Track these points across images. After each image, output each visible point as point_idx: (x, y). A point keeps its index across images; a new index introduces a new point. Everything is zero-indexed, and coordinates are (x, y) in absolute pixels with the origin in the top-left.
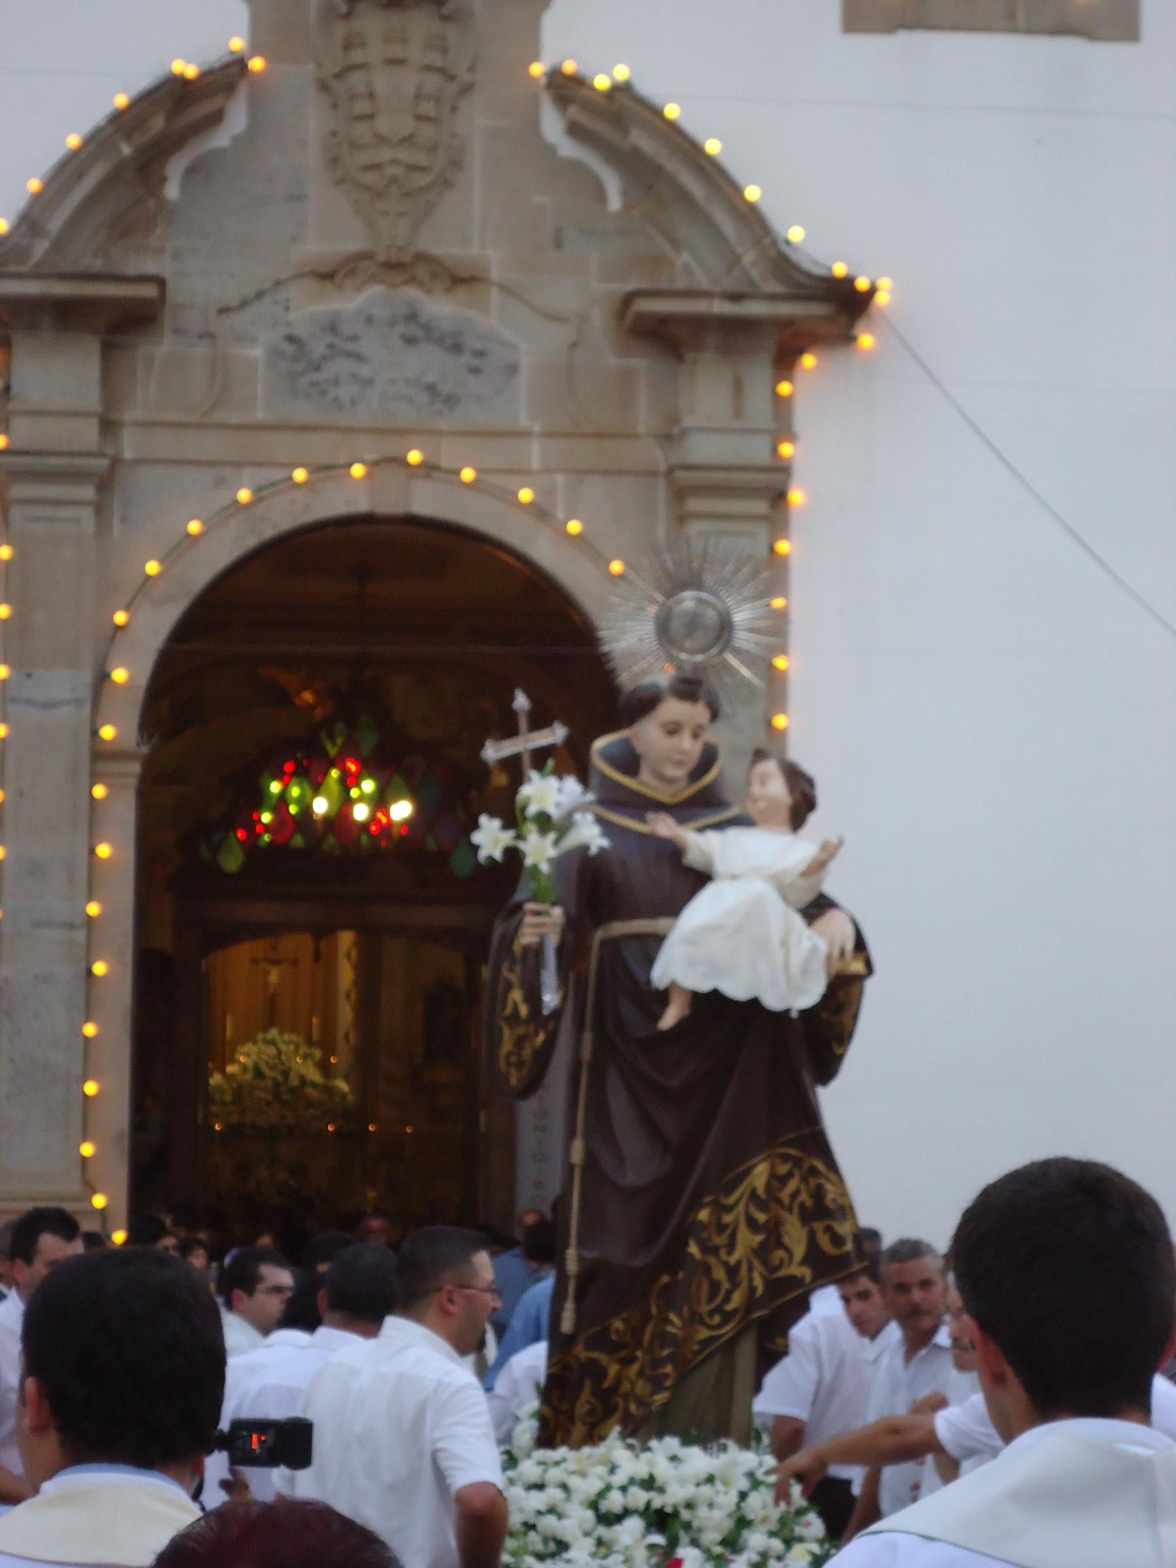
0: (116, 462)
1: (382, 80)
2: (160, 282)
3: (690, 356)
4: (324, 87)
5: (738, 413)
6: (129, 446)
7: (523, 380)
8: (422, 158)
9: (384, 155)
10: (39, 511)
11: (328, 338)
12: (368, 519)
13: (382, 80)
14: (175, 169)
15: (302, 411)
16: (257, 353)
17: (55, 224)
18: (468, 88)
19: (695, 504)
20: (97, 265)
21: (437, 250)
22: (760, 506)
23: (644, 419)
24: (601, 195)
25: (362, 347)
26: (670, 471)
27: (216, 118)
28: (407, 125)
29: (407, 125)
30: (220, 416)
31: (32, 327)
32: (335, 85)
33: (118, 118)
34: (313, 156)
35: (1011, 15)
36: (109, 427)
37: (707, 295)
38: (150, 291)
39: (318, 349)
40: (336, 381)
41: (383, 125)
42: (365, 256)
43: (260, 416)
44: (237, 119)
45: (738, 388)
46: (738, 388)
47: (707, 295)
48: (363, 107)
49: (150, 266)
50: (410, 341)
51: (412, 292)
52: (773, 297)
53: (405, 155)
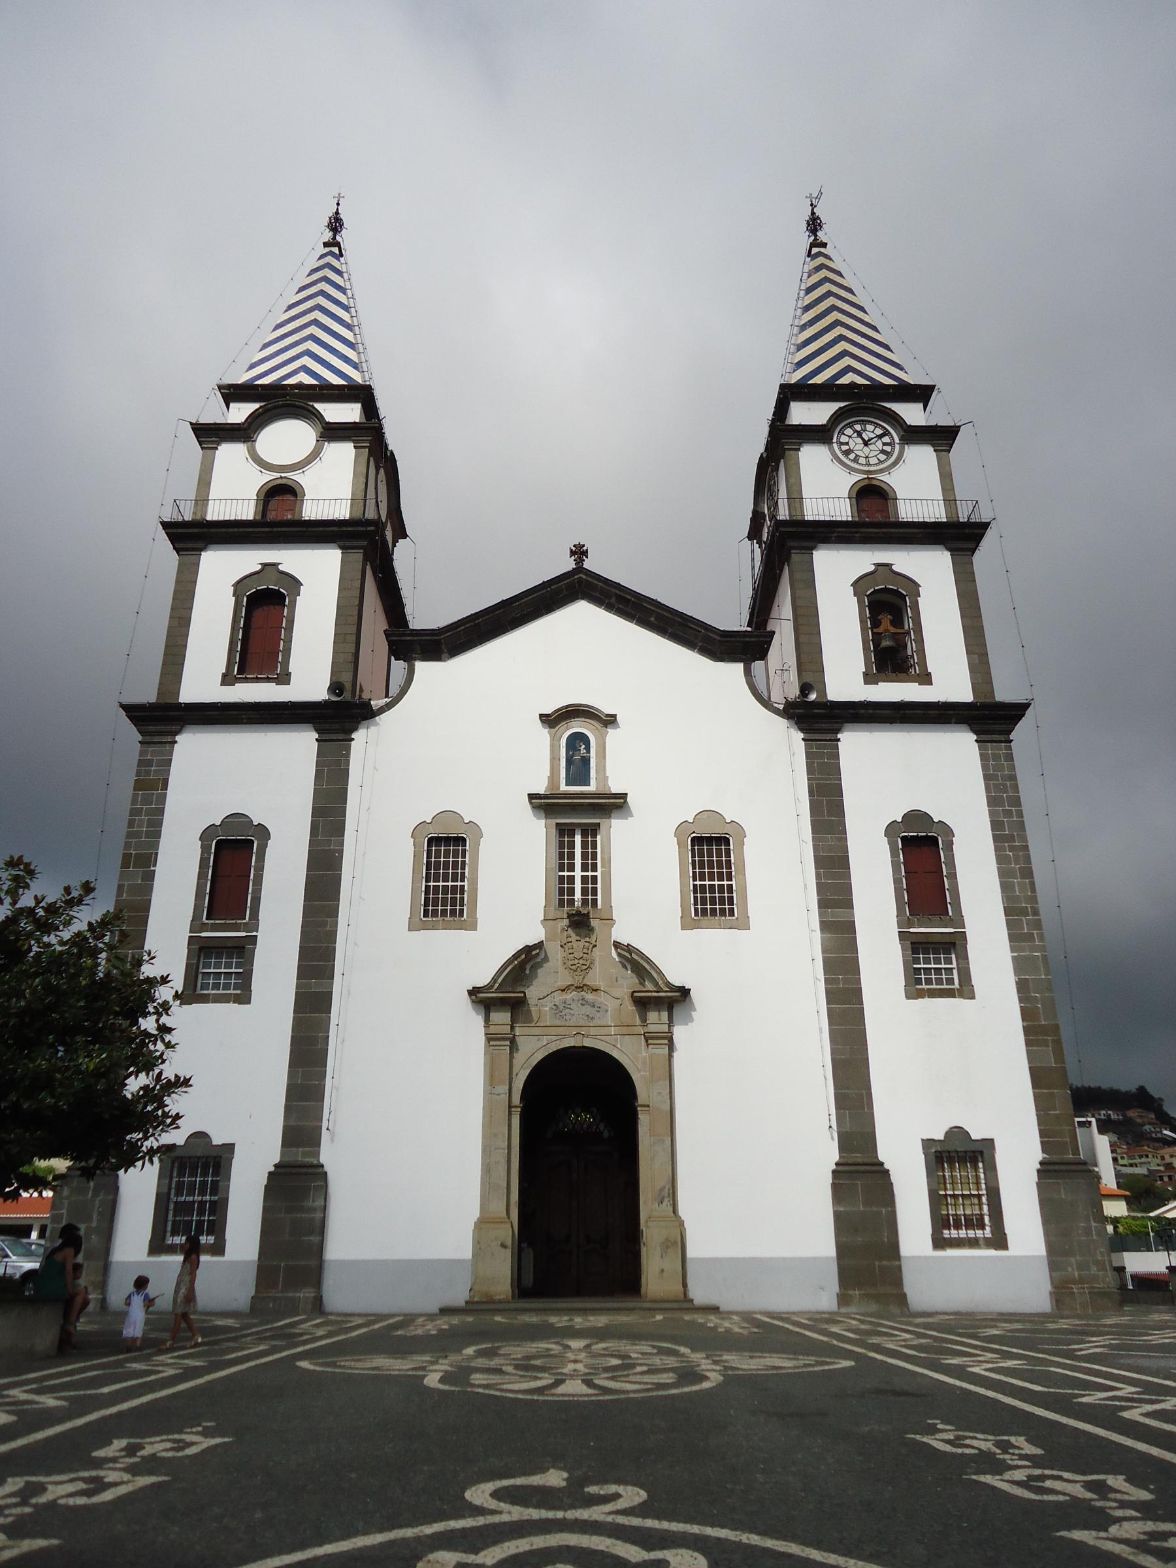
0: (514, 1035)
1: (575, 944)
2: (524, 993)
3: (648, 1006)
4: (562, 946)
5: (660, 1020)
6: (518, 1031)
7: (609, 1013)
8: (585, 962)
9: (577, 961)
10: (497, 1048)
11: (564, 1005)
12: (574, 1047)
13: (575, 944)
14: (528, 967)
15: (558, 1023)
16: (547, 1009)
17: (500, 980)
18: (595, 946)
19: (650, 1042)
20: (510, 989)
21: (588, 983)
22: (666, 1042)
23: (638, 1022)
24: (626, 968)
25: (571, 1007)
26: (644, 1035)
27: (538, 954)
28: (582, 955)
29: (582, 955)
30: (537, 1025)
31: (495, 1005)
32: (565, 946)
33: (516, 956)
34: (560, 963)
35: (720, 925)
36: (512, 1028)
37: (651, 992)
38: (522, 995)
39: (561, 1007)
40: (566, 1015)
41: (576, 955)
42: (573, 985)
43: (548, 1024)
44: (542, 956)
45: (659, 1015)
46: (659, 1015)
47: (651, 992)
48: (571, 951)
49: (522, 990)
50: (582, 1005)
51: (583, 993)
52: (666, 991)
53: (581, 961)
